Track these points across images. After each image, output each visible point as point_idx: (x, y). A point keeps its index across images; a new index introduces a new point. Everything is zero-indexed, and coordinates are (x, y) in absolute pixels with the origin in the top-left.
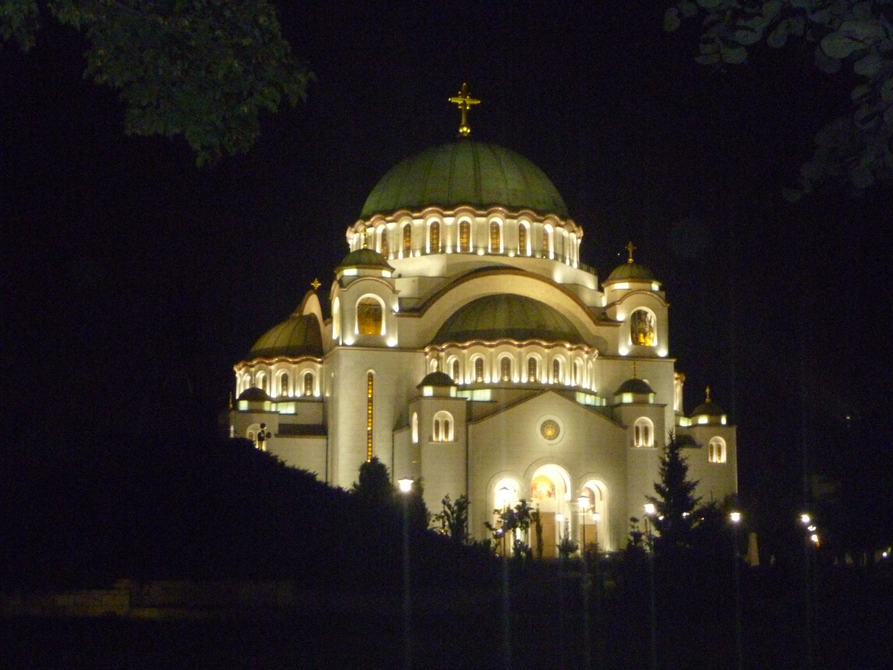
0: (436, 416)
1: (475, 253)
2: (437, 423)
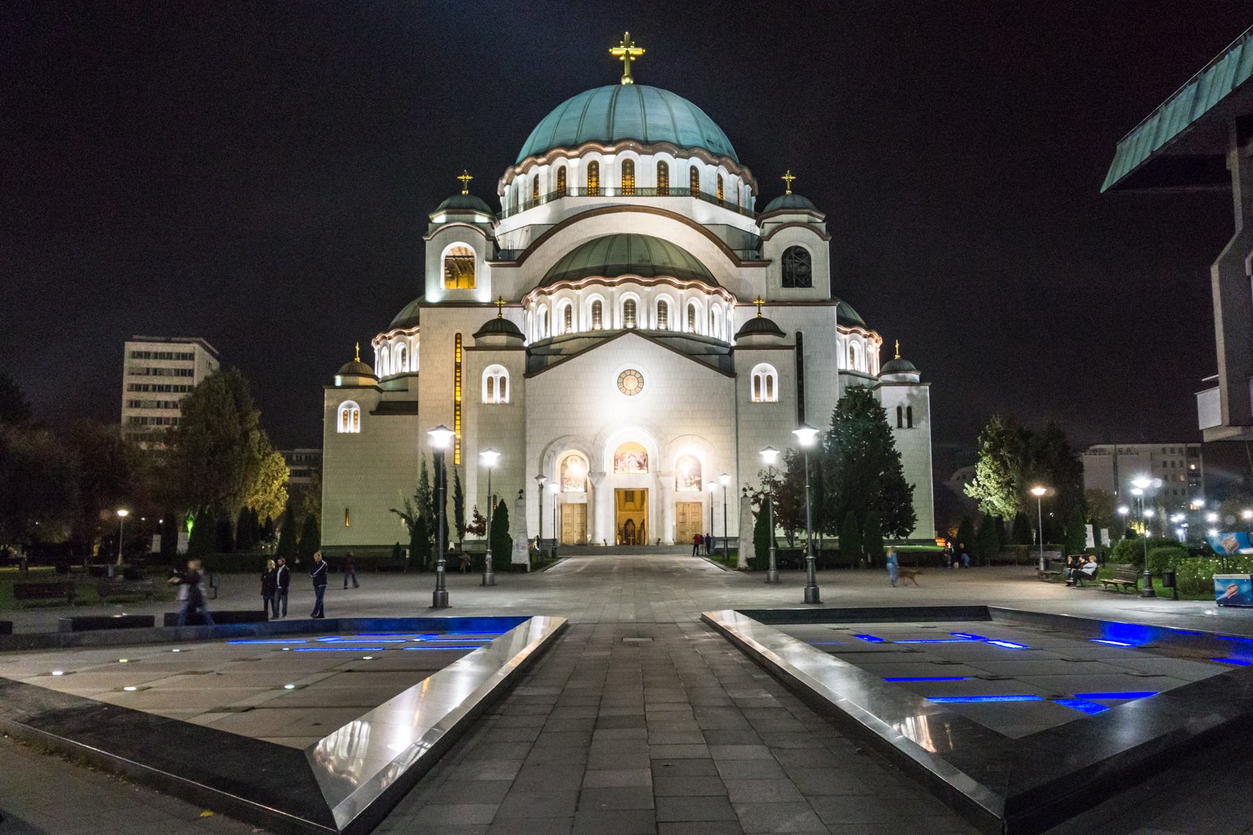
0: (487, 373)
2: (490, 381)
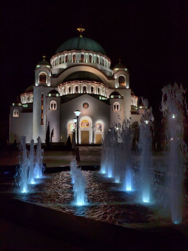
0: (52, 102)
1: (77, 62)
